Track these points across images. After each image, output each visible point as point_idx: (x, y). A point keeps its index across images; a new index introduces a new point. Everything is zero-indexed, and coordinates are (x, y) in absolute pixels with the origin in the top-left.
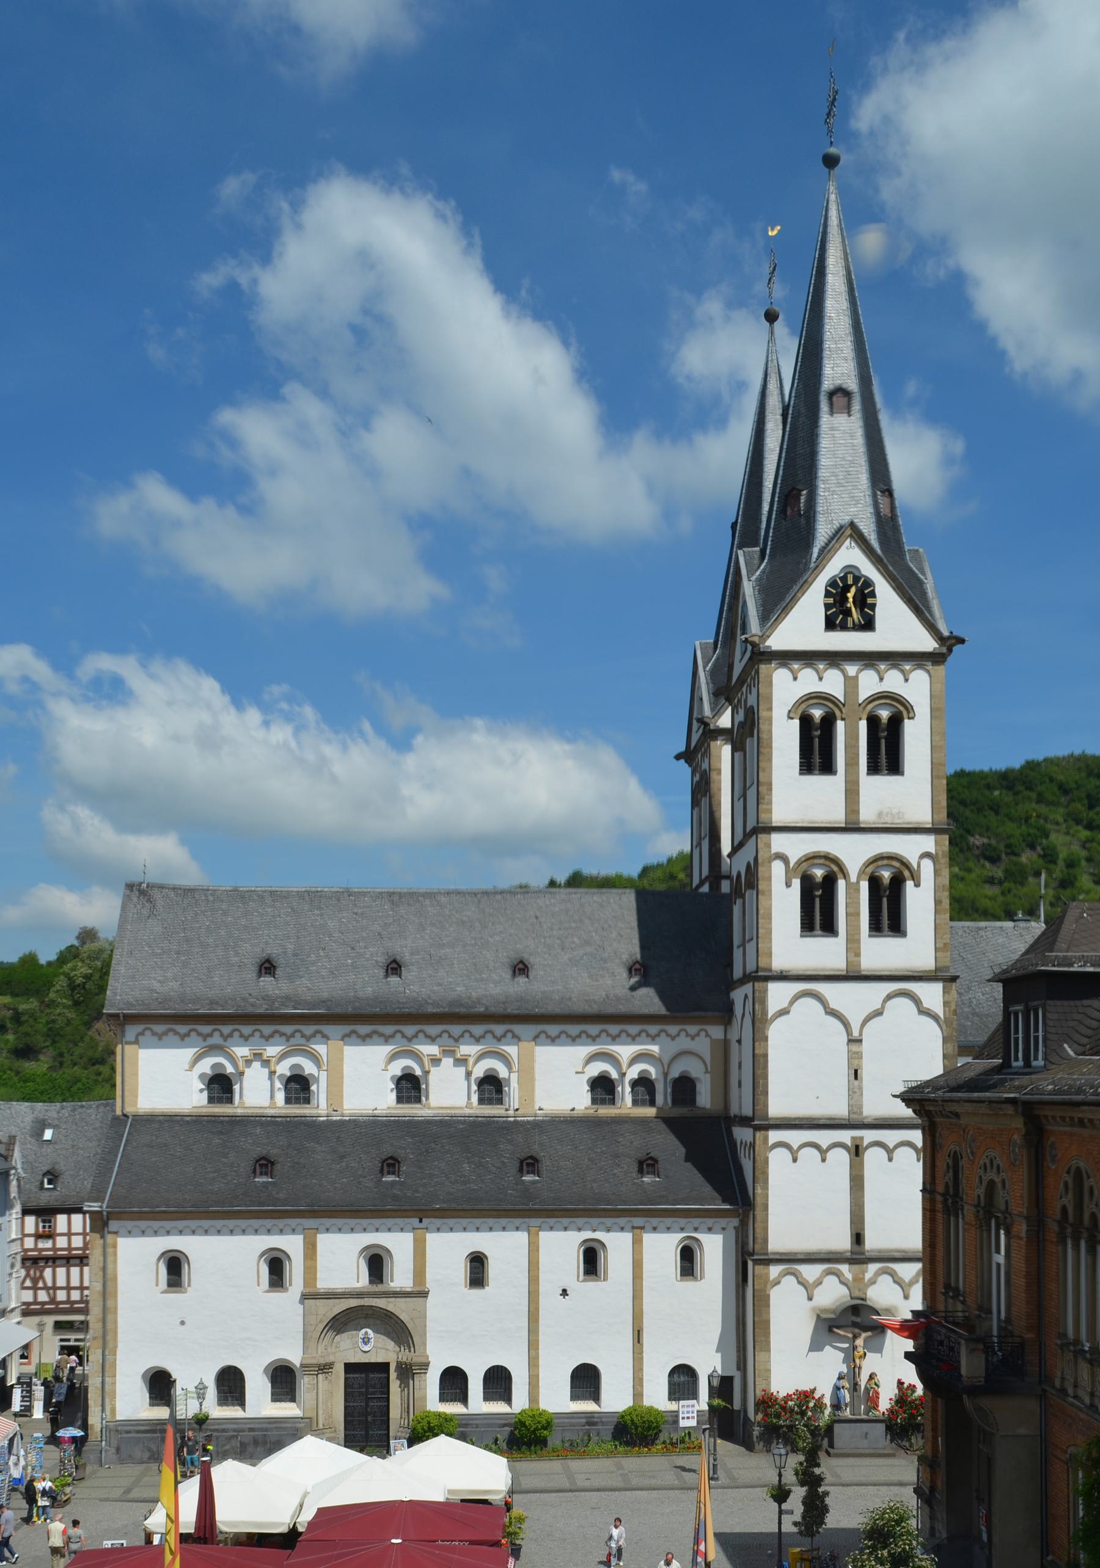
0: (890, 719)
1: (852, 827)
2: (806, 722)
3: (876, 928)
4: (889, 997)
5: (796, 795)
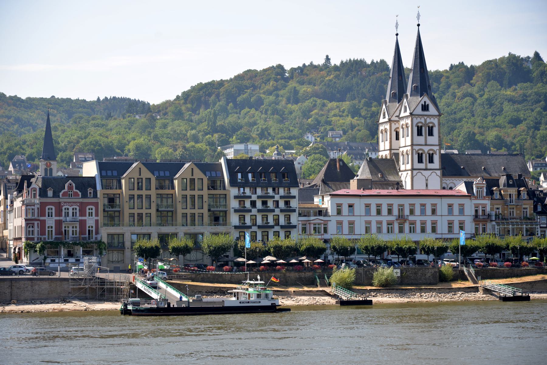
1: (426, 145)
2: (418, 127)
3: (430, 162)
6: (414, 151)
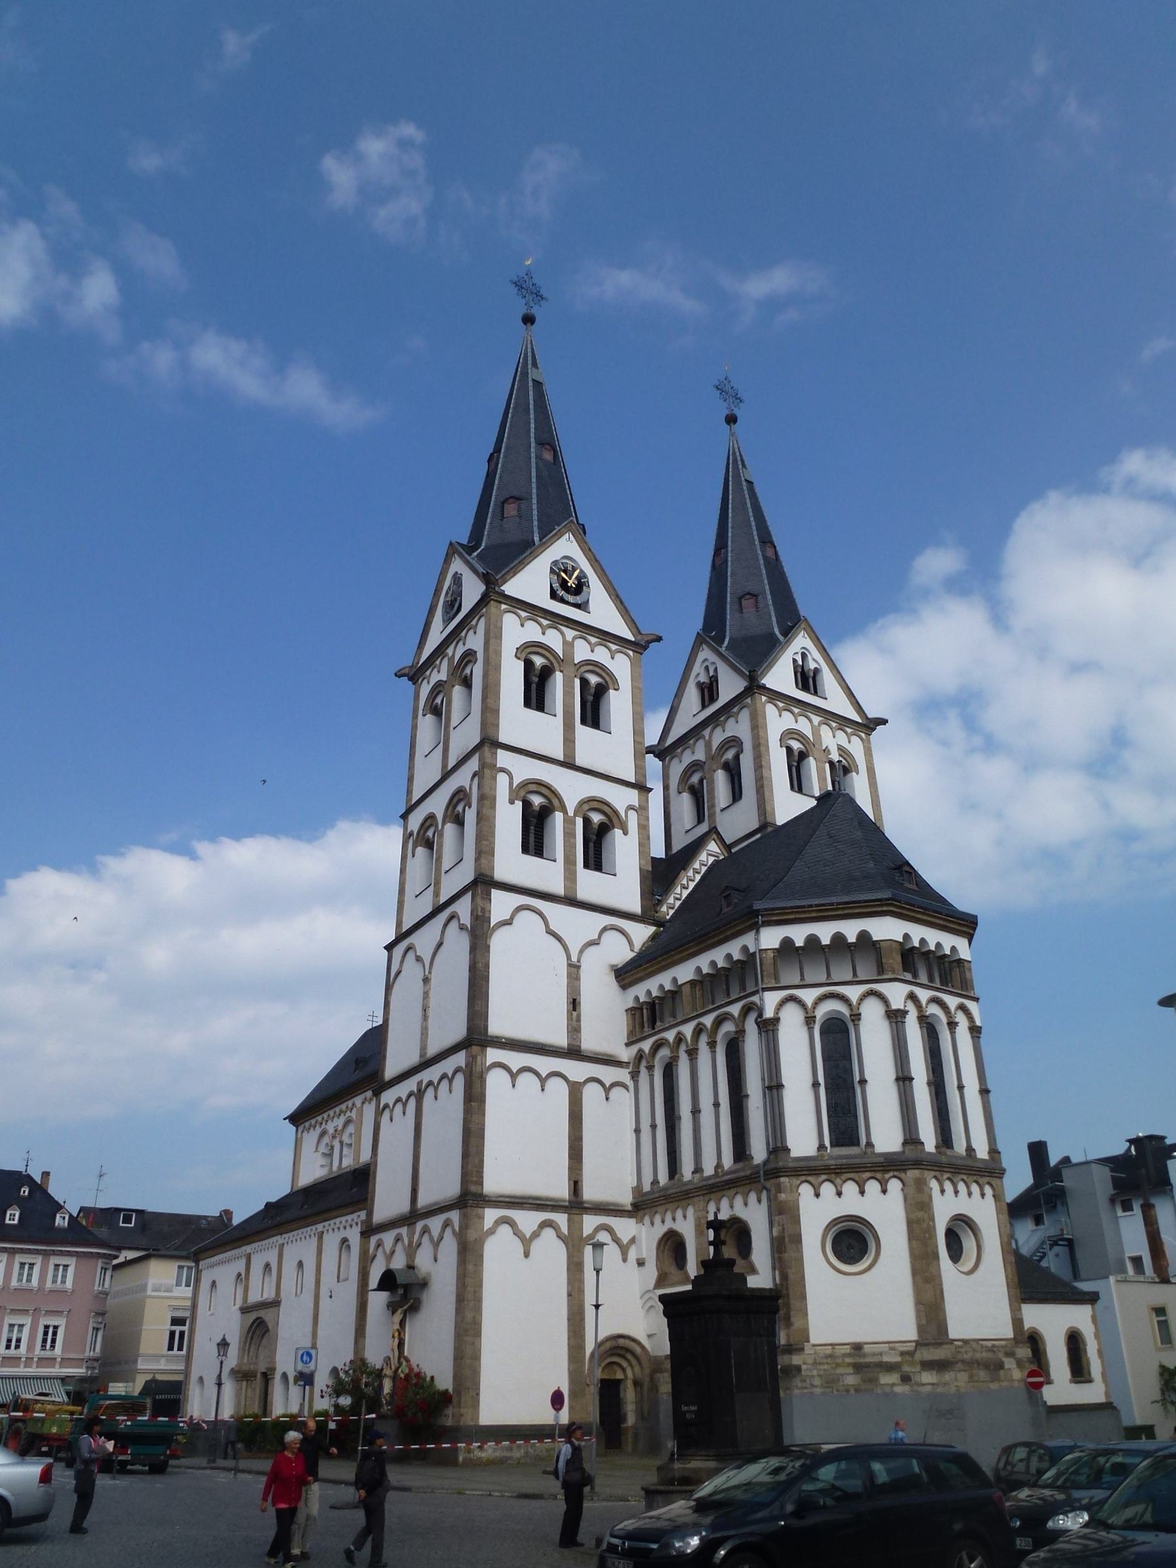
0: (598, 685)
1: (569, 764)
2: (529, 665)
4: (605, 929)
5: (517, 722)
6: (502, 780)
